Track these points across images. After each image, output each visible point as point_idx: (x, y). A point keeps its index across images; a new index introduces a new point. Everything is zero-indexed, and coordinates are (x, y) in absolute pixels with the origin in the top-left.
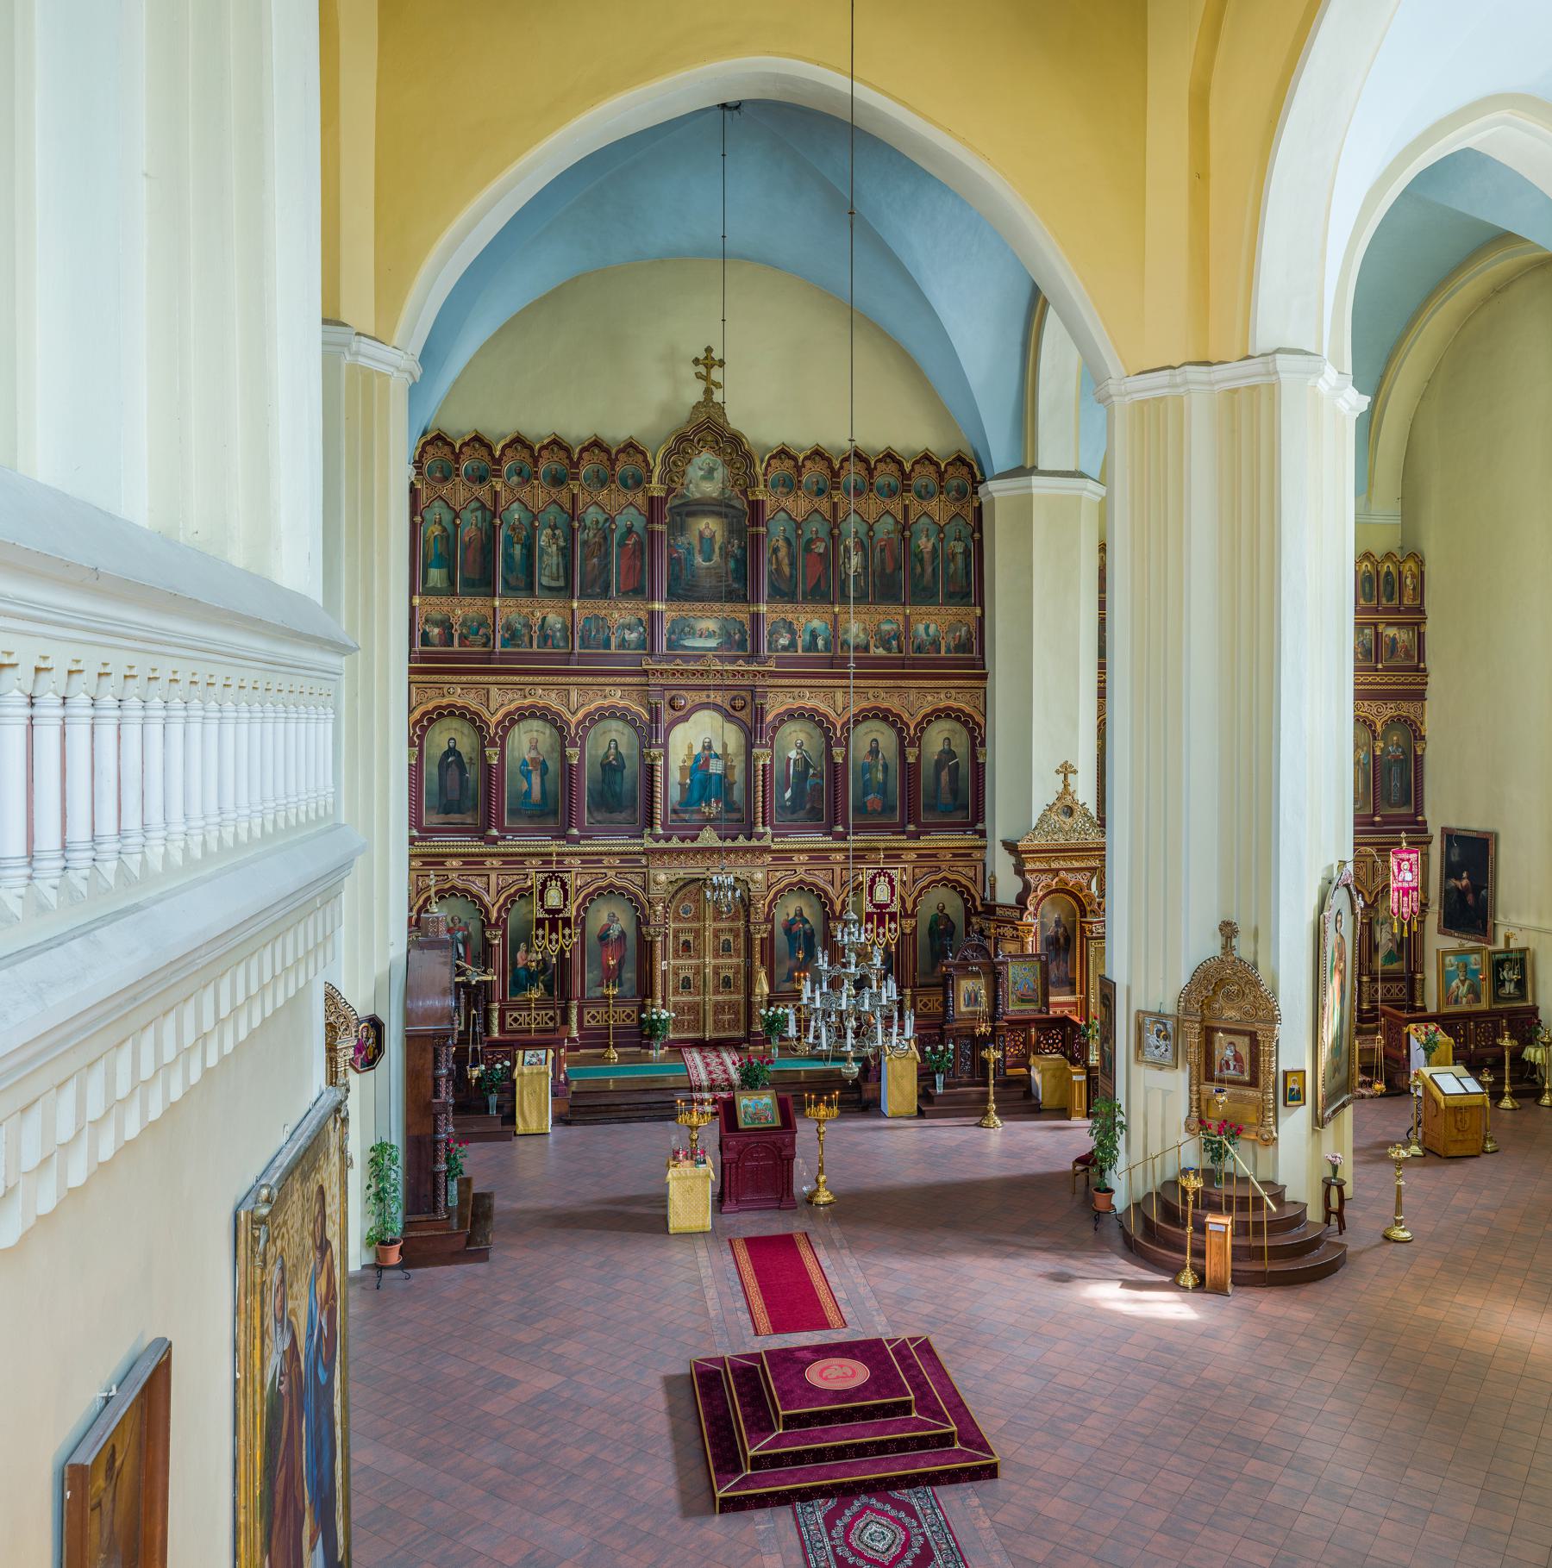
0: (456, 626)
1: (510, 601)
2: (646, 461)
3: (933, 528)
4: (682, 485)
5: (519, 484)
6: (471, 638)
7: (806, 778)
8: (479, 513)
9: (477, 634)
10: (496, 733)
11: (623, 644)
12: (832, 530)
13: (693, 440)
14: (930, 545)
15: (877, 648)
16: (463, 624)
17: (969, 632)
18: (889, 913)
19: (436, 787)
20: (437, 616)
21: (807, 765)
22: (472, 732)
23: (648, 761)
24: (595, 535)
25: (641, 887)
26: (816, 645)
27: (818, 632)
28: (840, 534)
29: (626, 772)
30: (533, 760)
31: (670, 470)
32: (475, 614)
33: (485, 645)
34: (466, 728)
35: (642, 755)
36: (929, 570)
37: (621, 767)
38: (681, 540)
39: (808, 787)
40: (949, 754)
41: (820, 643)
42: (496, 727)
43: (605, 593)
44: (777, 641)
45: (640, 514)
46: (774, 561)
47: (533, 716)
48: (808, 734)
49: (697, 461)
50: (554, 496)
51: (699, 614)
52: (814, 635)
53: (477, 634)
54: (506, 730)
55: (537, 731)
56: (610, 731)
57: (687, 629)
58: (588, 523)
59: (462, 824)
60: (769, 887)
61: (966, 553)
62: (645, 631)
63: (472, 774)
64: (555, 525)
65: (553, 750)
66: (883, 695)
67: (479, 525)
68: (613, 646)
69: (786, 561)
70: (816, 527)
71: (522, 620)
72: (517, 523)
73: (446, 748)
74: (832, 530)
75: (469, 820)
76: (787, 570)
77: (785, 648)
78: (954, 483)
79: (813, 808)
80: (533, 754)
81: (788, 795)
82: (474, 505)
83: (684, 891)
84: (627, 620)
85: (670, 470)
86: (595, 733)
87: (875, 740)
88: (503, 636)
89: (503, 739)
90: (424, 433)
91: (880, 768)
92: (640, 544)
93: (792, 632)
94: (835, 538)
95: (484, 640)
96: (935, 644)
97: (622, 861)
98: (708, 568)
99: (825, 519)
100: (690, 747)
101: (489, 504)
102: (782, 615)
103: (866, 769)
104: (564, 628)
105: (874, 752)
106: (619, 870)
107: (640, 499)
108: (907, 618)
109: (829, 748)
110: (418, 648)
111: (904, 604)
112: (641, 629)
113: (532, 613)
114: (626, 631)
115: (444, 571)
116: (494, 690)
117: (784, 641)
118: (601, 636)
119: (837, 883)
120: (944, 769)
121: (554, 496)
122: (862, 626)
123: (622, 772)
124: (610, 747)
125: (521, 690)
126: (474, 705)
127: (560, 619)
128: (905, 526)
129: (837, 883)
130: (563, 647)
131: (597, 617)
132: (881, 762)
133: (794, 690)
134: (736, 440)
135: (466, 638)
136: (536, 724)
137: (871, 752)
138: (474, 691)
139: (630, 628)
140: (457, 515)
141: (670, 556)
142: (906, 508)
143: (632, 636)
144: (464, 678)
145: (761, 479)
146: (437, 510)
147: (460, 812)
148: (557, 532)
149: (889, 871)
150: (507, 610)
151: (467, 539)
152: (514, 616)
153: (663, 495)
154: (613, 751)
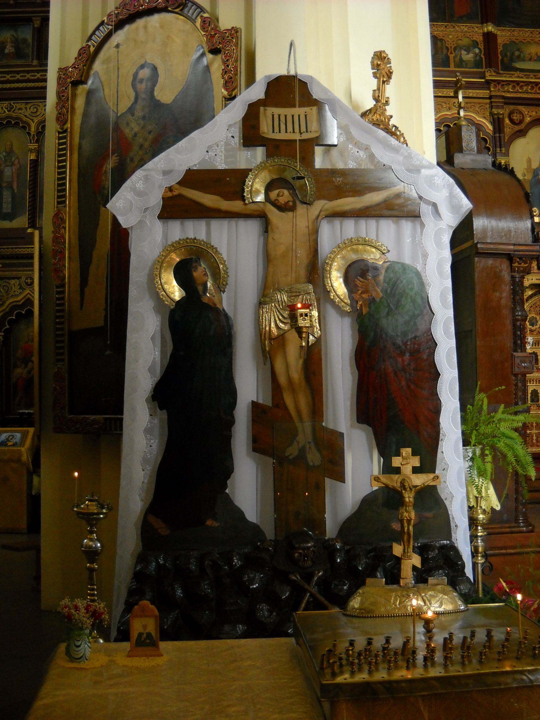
57: (517, 53)
68: (452, 64)
100: (529, 161)
112: (477, 51)
114: (464, 52)
139: (468, 50)
143: (468, 57)
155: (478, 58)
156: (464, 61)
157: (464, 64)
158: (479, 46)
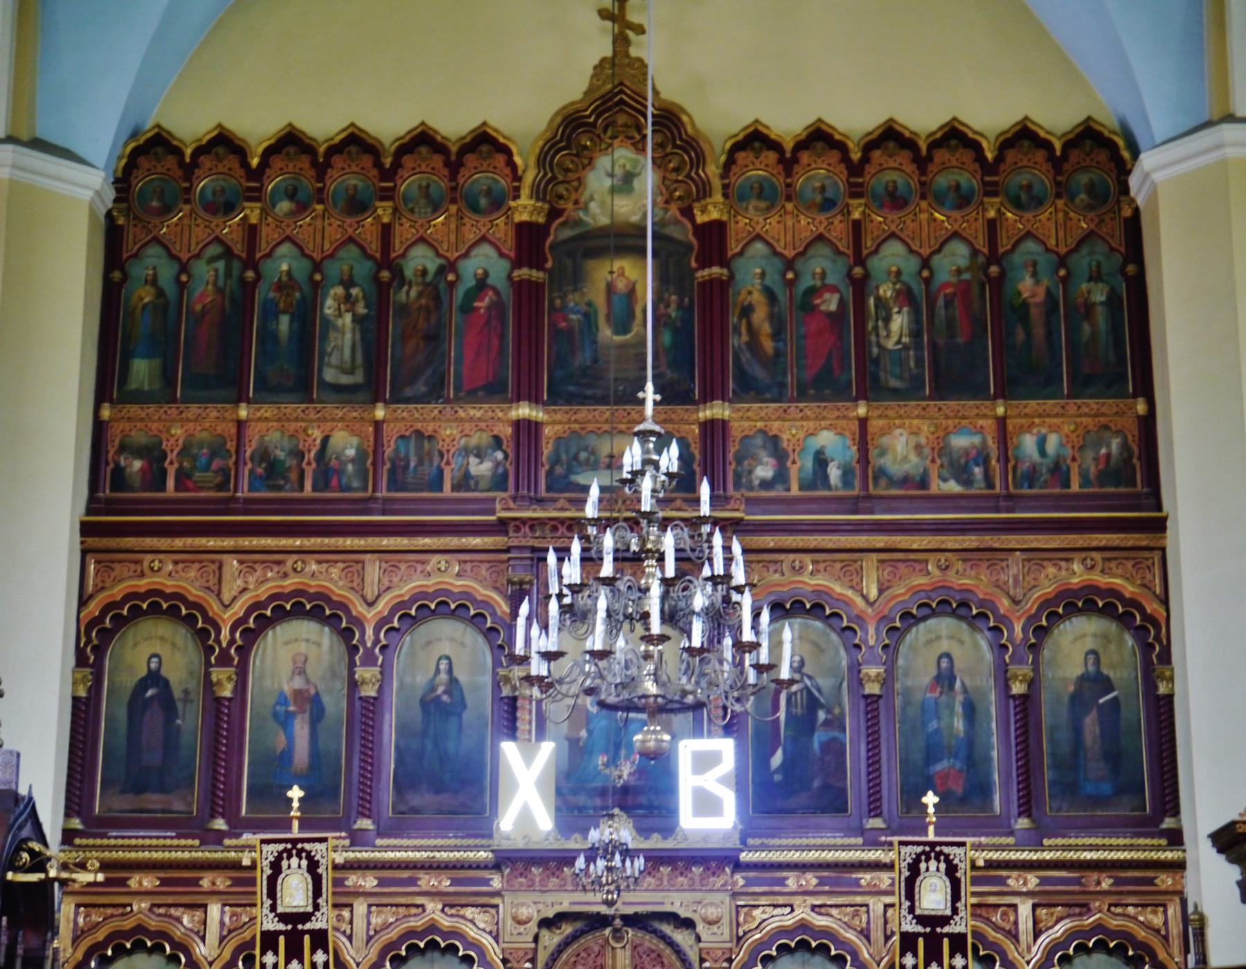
0: (172, 456)
1: (267, 411)
2: (511, 164)
3: (1044, 261)
4: (576, 202)
5: (291, 214)
6: (198, 475)
7: (811, 728)
8: (221, 265)
9: (207, 467)
10: (232, 641)
11: (465, 481)
12: (850, 269)
13: (594, 124)
14: (1041, 295)
15: (945, 480)
16: (185, 451)
17: (1125, 446)
18: (951, 936)
19: (121, 741)
20: (139, 437)
21: (813, 704)
22: (191, 644)
23: (506, 691)
24: (420, 295)
25: (490, 933)
26: (826, 477)
27: (828, 453)
28: (867, 276)
29: (467, 716)
30: (298, 693)
31: (554, 178)
32: (205, 435)
33: (222, 486)
34: (181, 635)
35: (496, 686)
36: (1039, 331)
37: (459, 704)
38: (573, 300)
39: (816, 745)
40: (1095, 682)
41: (834, 473)
42: (233, 630)
43: (435, 393)
44: (750, 472)
45: (501, 255)
46: (743, 330)
47: (298, 612)
48: (815, 644)
49: (603, 162)
50: (350, 230)
51: (606, 427)
52: (821, 461)
53: (207, 467)
54: (251, 636)
55: (308, 641)
56: (439, 640)
57: (583, 455)
58: (409, 273)
59: (164, 811)
60: (739, 939)
61: (1113, 301)
62: (506, 457)
63: (191, 720)
64: (351, 277)
65: (334, 675)
66: (959, 566)
67: (221, 283)
68: (447, 485)
69: (766, 328)
70: (820, 265)
71: (286, 443)
72: (284, 279)
73: (143, 672)
74: (850, 269)
75: (178, 806)
76: (768, 345)
77: (765, 484)
78: (1083, 178)
79: (826, 787)
80: (298, 683)
81: (777, 759)
82: (214, 250)
83: (570, 951)
84: (474, 441)
85: (554, 178)
86: (412, 643)
87: (948, 655)
88: (251, 472)
89: (244, 651)
90: (134, 135)
91: (959, 709)
92: (498, 307)
93: (781, 456)
94: (860, 286)
95: (219, 479)
96: (1059, 472)
97: (455, 882)
98: (622, 346)
99: (838, 252)
101: (238, 249)
102: (760, 424)
103: (931, 710)
104: (361, 456)
105: (945, 679)
106: (450, 900)
107: (501, 228)
108: (1002, 422)
109: (855, 668)
110: (106, 493)
111: (995, 397)
113: (305, 430)
114: (473, 460)
115: (157, 362)
116: (232, 563)
117: (764, 471)
118: (428, 470)
119: (877, 934)
120: (1088, 712)
121: (350, 230)
122: (913, 439)
123: (460, 716)
124: (438, 671)
125: (279, 563)
126: (194, 592)
127: (355, 441)
128: (994, 257)
129: (877, 934)
130: (356, 490)
131: (418, 433)
132: (960, 698)
133: (782, 557)
134: (669, 119)
135: (189, 476)
136: (305, 629)
137: (938, 679)
138: (197, 566)
139: (480, 455)
140: (184, 268)
141: (552, 325)
142: (992, 225)
143: (481, 468)
144: (179, 543)
145: (717, 183)
146: (150, 262)
147: (163, 789)
148: (355, 291)
149: (946, 850)
150: (262, 426)
151: (198, 307)
152: (274, 437)
153: (541, 220)
154: (443, 677)
155: (500, 470)
156: (472, 477)
157: (472, 483)
158: (504, 447)
